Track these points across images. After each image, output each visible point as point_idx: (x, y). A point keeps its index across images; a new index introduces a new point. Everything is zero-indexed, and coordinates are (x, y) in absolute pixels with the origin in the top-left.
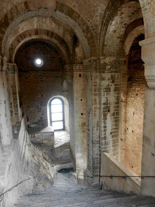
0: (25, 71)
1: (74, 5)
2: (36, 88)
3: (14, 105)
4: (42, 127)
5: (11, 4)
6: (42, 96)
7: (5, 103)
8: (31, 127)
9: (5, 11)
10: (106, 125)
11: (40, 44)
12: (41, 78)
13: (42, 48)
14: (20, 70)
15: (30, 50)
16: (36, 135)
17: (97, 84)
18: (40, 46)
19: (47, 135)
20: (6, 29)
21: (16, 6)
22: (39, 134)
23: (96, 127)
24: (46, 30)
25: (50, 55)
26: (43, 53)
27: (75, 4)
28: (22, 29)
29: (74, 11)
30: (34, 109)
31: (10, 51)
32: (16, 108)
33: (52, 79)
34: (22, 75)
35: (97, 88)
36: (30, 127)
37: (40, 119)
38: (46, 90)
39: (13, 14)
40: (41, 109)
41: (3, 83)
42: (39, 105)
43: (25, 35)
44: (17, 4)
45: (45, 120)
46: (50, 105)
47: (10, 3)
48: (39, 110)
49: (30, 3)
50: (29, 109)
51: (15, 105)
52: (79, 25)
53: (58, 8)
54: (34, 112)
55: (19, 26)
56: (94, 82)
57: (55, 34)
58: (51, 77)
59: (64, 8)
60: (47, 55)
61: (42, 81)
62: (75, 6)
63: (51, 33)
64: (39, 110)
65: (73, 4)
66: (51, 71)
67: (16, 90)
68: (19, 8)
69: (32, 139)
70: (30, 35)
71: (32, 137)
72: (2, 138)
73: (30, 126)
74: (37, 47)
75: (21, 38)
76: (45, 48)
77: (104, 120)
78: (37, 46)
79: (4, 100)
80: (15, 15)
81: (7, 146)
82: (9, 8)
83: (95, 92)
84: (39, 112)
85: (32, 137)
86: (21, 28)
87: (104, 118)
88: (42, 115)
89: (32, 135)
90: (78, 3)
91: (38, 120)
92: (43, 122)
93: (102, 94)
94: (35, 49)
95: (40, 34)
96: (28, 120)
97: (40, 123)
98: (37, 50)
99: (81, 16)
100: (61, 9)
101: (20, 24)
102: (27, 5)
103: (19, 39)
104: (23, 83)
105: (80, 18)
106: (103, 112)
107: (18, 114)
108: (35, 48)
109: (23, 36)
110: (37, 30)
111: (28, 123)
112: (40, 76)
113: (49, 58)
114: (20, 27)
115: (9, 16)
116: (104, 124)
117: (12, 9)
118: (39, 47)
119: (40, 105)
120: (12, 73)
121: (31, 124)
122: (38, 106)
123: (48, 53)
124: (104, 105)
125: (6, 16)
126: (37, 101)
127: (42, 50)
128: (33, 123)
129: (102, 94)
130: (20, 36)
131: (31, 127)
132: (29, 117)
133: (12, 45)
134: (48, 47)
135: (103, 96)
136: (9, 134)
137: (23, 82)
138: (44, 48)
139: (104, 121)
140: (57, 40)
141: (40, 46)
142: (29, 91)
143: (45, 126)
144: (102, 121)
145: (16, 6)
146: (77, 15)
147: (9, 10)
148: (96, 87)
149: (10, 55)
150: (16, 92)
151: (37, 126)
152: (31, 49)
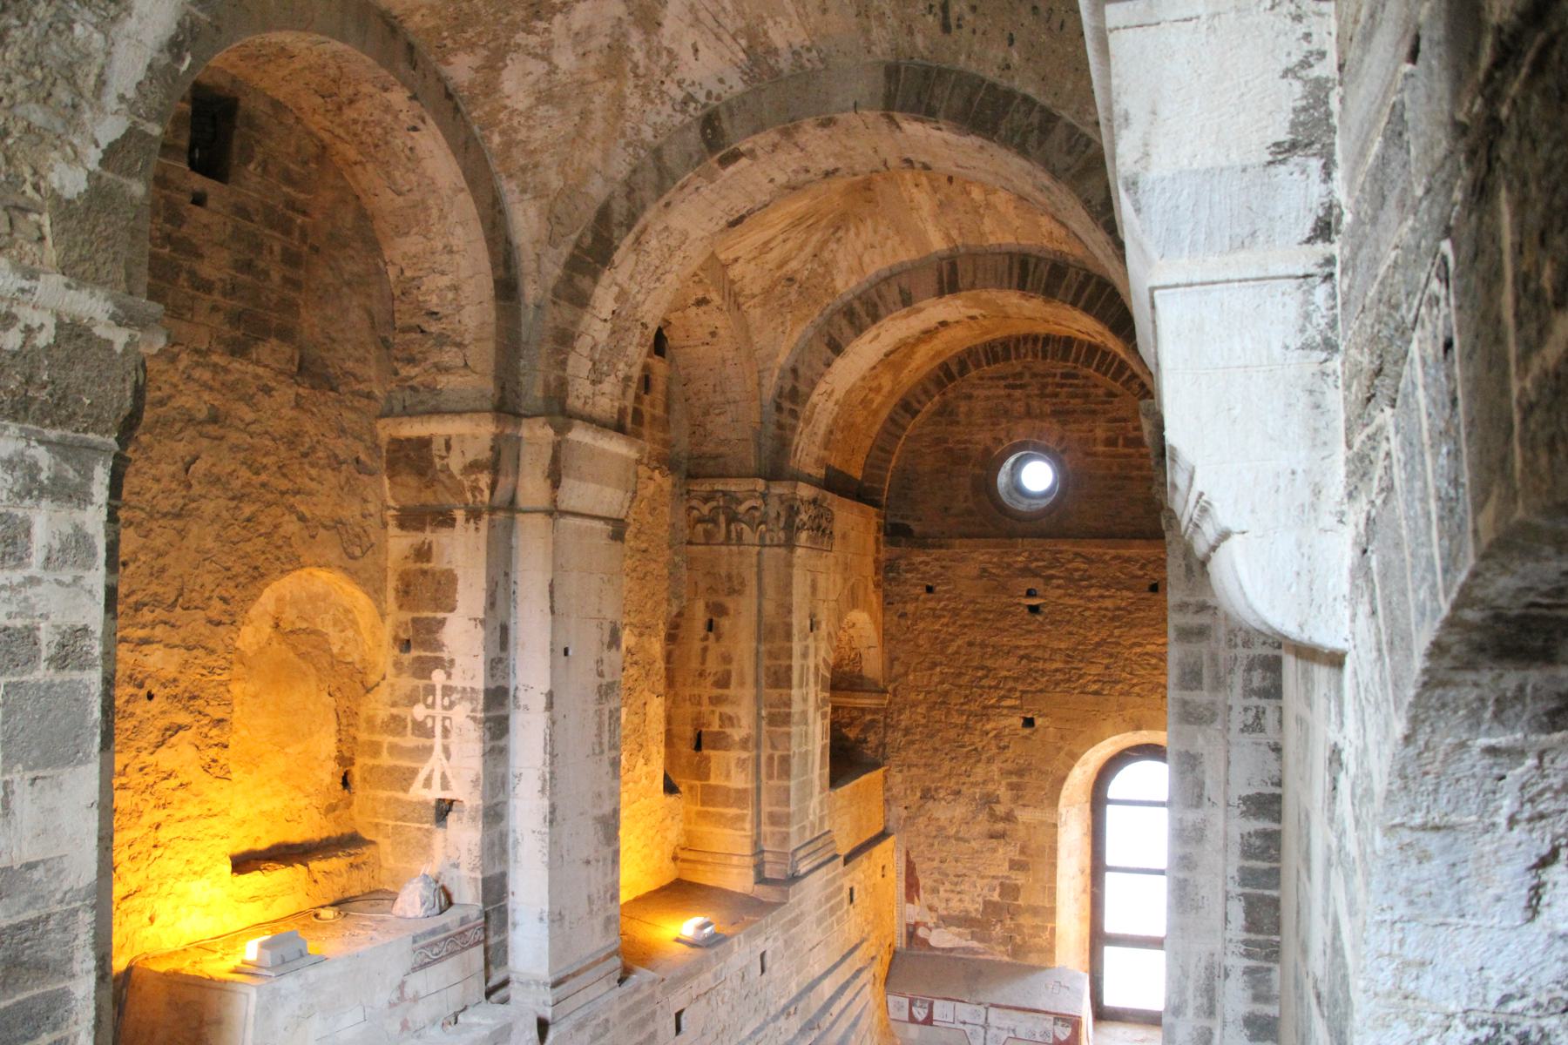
0: (922, 542)
1: (1000, 60)
2: (989, 663)
3: (771, 758)
4: (1000, 964)
5: (628, 144)
6: (1029, 722)
7: (550, 706)
8: (933, 943)
9: (597, 189)
10: (1272, 1010)
11: (1035, 356)
12: (1030, 593)
13: (1050, 380)
14: (895, 533)
15: (970, 397)
16: (941, 1010)
17: (1204, 619)
18: (1039, 367)
19: (1022, 1033)
20: (595, 282)
21: (657, 153)
22: (964, 1011)
23: (1190, 1012)
24: (1011, 255)
25: (1115, 420)
26: (1054, 413)
27: (1001, 55)
28: (851, 270)
29: (1010, 95)
30: (960, 810)
31: (779, 408)
32: (780, 777)
33: (1108, 603)
34: (903, 562)
35: (1214, 658)
36: (925, 942)
37: (996, 897)
38: (1059, 676)
39: (637, 195)
40: (1009, 818)
41: (551, 586)
42: (1003, 792)
43: (875, 305)
44: (660, 140)
45: (1035, 911)
46: (1098, 800)
47: (622, 142)
48: (1000, 826)
49: (731, 115)
50: (930, 804)
51: (777, 754)
52: (1135, 183)
53: (899, 101)
54: (959, 839)
55: (826, 255)
56: (1182, 607)
57: (1072, 271)
58: (1107, 587)
59: (937, 91)
60: (1085, 426)
61: (1034, 610)
62: (1008, 67)
63: (1044, 269)
64: (1000, 826)
65: (991, 54)
66: (1106, 535)
67: (790, 657)
68: (672, 157)
69: (914, 1031)
70: (907, 300)
71: (912, 1020)
72: (515, 925)
73: (921, 932)
74: (1020, 375)
75: (851, 323)
76: (1075, 376)
77: (1249, 955)
78: (1019, 369)
79: (546, 688)
80: (648, 194)
81: (534, 988)
82: (620, 166)
83: (1188, 695)
84: (994, 842)
85: (912, 1020)
86: (843, 265)
87: (1259, 945)
88: (1015, 865)
89: (911, 1004)
90: (1016, 43)
91: (987, 903)
92: (1018, 926)
93: (1237, 709)
94: (1002, 392)
95: (973, 286)
96: (912, 888)
97: (998, 930)
98: (1018, 393)
99: (1067, 116)
100: (919, 101)
101: (833, 246)
102: (714, 129)
103: (836, 335)
104: (902, 622)
105: (1059, 135)
106: (1244, 882)
107: (788, 824)
108: (1003, 383)
109: (863, 314)
110: (953, 265)
111: (914, 912)
112: (1025, 571)
113: (1101, 448)
114: (834, 261)
115: (619, 208)
116: (1257, 998)
117: (634, 171)
118: (1034, 375)
119: (1012, 787)
120: (779, 546)
121: (930, 919)
122: (989, 800)
123: (1094, 412)
124: (1256, 816)
125: (604, 214)
126: (990, 760)
127: (1049, 390)
128: (946, 921)
129: (1237, 709)
130: (849, 313)
131: (931, 948)
132: (922, 867)
133: (794, 371)
134: (1097, 370)
135: (1246, 728)
136: (546, 908)
137: (903, 615)
138: (1065, 376)
139: (1249, 971)
140: (1087, 309)
141: (1039, 367)
142: (936, 679)
143: (1033, 959)
144: (1238, 964)
145: (657, 153)
146: (1035, 118)
147: (619, 177)
148: (1201, 649)
149: (777, 432)
150: (789, 668)
151: (974, 944)
152: (976, 393)
